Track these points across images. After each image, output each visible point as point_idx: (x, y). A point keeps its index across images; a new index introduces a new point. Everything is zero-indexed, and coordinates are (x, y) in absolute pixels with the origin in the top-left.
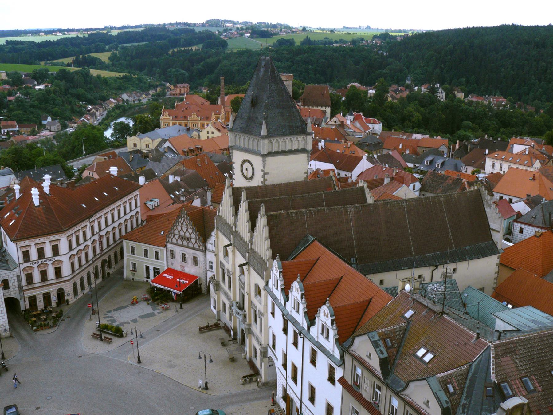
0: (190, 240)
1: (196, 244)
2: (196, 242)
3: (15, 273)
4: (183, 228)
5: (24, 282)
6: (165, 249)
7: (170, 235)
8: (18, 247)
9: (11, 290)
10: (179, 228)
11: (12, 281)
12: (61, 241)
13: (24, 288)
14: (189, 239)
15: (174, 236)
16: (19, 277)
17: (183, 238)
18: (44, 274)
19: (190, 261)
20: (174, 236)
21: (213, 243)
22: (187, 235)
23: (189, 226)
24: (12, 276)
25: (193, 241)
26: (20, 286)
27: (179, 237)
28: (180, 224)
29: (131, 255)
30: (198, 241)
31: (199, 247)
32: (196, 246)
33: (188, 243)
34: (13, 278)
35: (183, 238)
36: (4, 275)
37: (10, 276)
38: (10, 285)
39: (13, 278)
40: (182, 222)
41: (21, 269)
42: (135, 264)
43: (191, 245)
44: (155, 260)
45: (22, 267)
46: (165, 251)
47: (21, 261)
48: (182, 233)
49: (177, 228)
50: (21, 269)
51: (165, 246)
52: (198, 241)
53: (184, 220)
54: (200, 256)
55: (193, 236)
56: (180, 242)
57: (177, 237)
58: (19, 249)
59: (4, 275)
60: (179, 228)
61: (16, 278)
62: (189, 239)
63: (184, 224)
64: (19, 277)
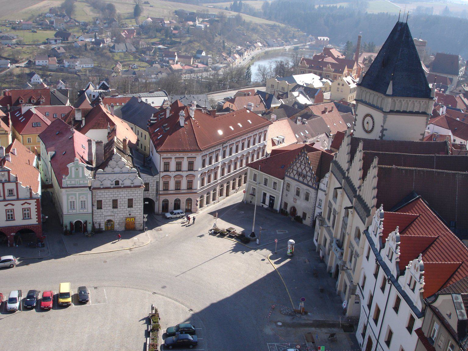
0: (306, 177)
1: (310, 182)
2: (311, 179)
3: (155, 179)
4: (302, 166)
5: (161, 187)
6: (283, 181)
8: (161, 158)
9: (150, 192)
10: (298, 165)
11: (151, 185)
12: (196, 159)
13: (161, 193)
14: (305, 177)
15: (292, 171)
16: (158, 183)
17: (300, 174)
18: (178, 184)
19: (302, 196)
20: (292, 171)
21: (326, 184)
23: (307, 165)
24: (153, 181)
25: (309, 178)
26: (157, 190)
27: (297, 173)
28: (299, 162)
29: (252, 181)
30: (312, 179)
31: (313, 184)
32: (310, 183)
33: (303, 180)
34: (153, 183)
35: (300, 174)
36: (147, 179)
37: (151, 181)
38: (150, 188)
39: (153, 183)
40: (301, 160)
41: (161, 177)
42: (254, 189)
43: (305, 182)
44: (272, 189)
45: (162, 174)
46: (282, 183)
47: (162, 169)
48: (300, 170)
49: (296, 165)
50: (161, 177)
51: (283, 179)
52: (312, 179)
53: (304, 159)
55: (309, 174)
56: (296, 177)
57: (295, 172)
58: (162, 160)
59: (147, 179)
60: (298, 165)
61: (155, 183)
62: (305, 177)
63: (303, 162)
64: (158, 183)
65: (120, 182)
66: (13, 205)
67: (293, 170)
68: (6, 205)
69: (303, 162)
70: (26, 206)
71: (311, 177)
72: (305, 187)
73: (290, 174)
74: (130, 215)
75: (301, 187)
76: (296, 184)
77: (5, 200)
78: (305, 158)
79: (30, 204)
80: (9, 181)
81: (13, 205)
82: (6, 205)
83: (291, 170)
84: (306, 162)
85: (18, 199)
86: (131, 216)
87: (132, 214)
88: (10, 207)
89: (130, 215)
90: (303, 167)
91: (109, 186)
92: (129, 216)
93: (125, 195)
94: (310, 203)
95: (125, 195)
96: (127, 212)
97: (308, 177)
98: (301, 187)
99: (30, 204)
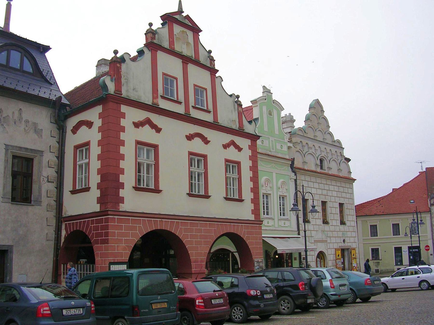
46: (428, 219)
65: (325, 164)
66: (206, 141)
68: (190, 137)
70: (232, 154)
74: (344, 241)
77: (186, 118)
79: (240, 149)
80: (197, 63)
81: (206, 141)
82: (190, 137)
85: (215, 126)
86: (346, 244)
87: (347, 240)
88: (197, 146)
89: (344, 241)
91: (313, 168)
92: (343, 244)
93: (335, 194)
95: (335, 194)
96: (340, 234)
99: (240, 149)
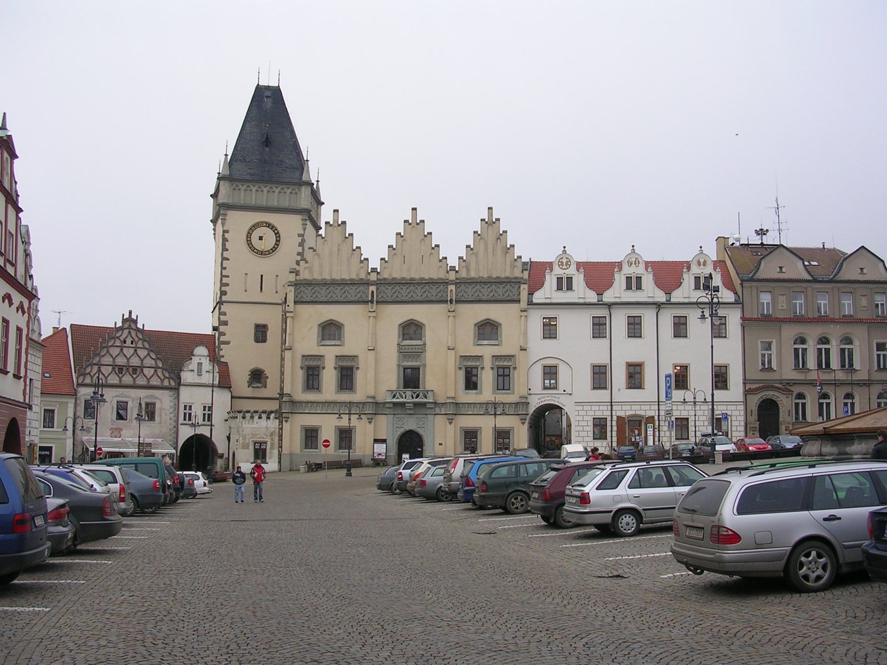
4: (125, 350)
6: (71, 403)
7: (88, 370)
20: (99, 371)
22: (135, 361)
25: (148, 372)
28: (118, 343)
31: (162, 381)
32: (155, 382)
46: (71, 406)
48: (121, 361)
52: (159, 372)
53: (130, 332)
54: (163, 400)
55: (149, 362)
60: (115, 351)
63: (129, 341)
67: (99, 365)
69: (129, 341)
71: (156, 368)
72: (142, 393)
73: (92, 377)
75: (129, 397)
76: (117, 394)
78: (133, 333)
83: (96, 368)
84: (136, 339)
90: (129, 352)
94: (160, 423)
97: (146, 371)
98: (129, 397)
